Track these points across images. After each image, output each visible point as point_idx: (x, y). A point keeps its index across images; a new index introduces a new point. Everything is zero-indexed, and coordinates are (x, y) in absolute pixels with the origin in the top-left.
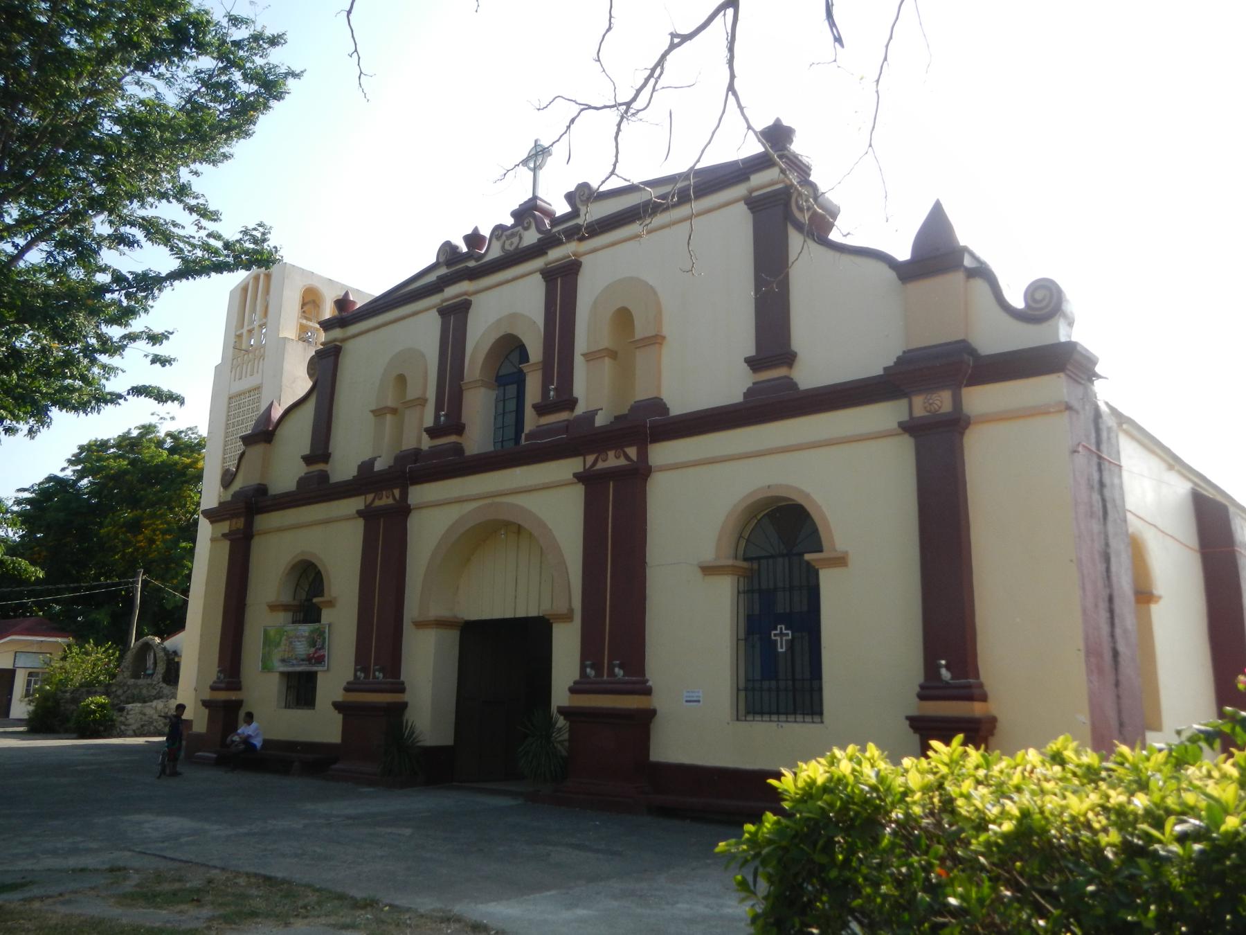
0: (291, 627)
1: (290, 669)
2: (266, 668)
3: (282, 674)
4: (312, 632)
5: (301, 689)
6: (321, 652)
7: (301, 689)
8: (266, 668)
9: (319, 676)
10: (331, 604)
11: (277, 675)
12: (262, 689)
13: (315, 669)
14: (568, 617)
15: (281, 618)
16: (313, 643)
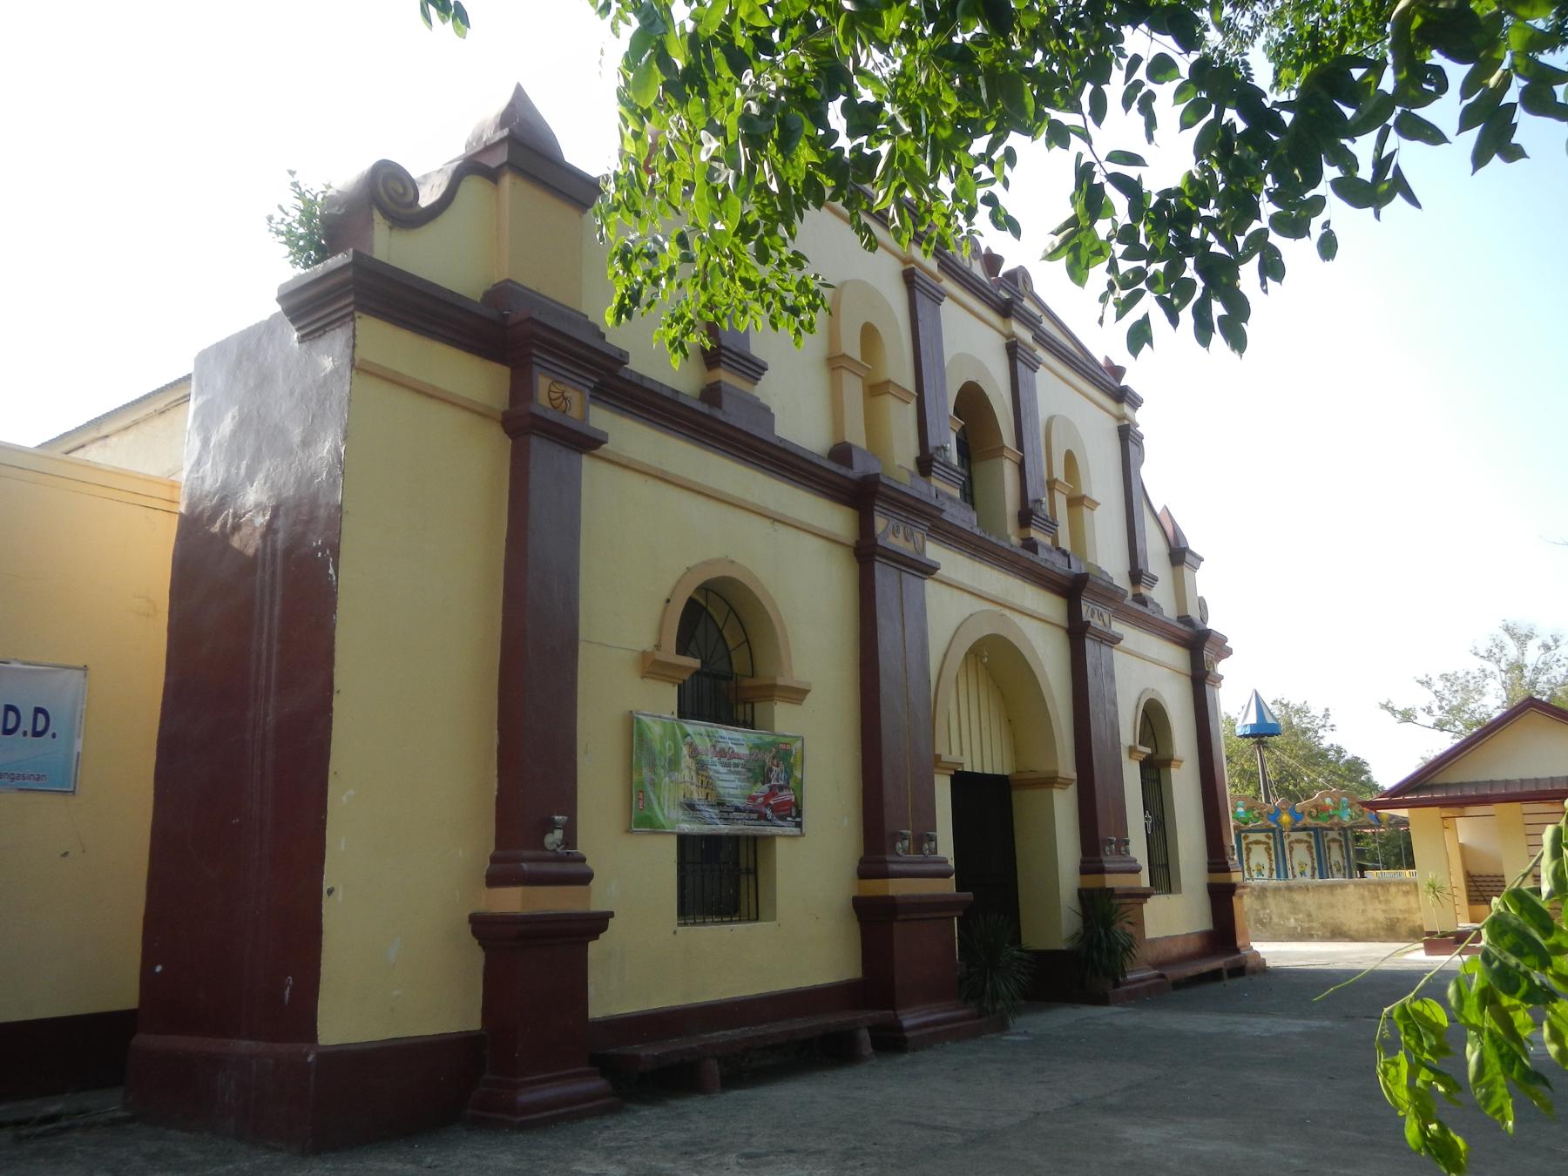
0: (696, 729)
1: (705, 829)
2: (641, 821)
3: (683, 840)
4: (757, 746)
5: (719, 878)
6: (787, 796)
7: (719, 878)
8: (641, 821)
9: (781, 846)
10: (797, 695)
11: (673, 843)
12: (631, 875)
13: (770, 830)
14: (1065, 783)
15: (666, 697)
16: (760, 773)
